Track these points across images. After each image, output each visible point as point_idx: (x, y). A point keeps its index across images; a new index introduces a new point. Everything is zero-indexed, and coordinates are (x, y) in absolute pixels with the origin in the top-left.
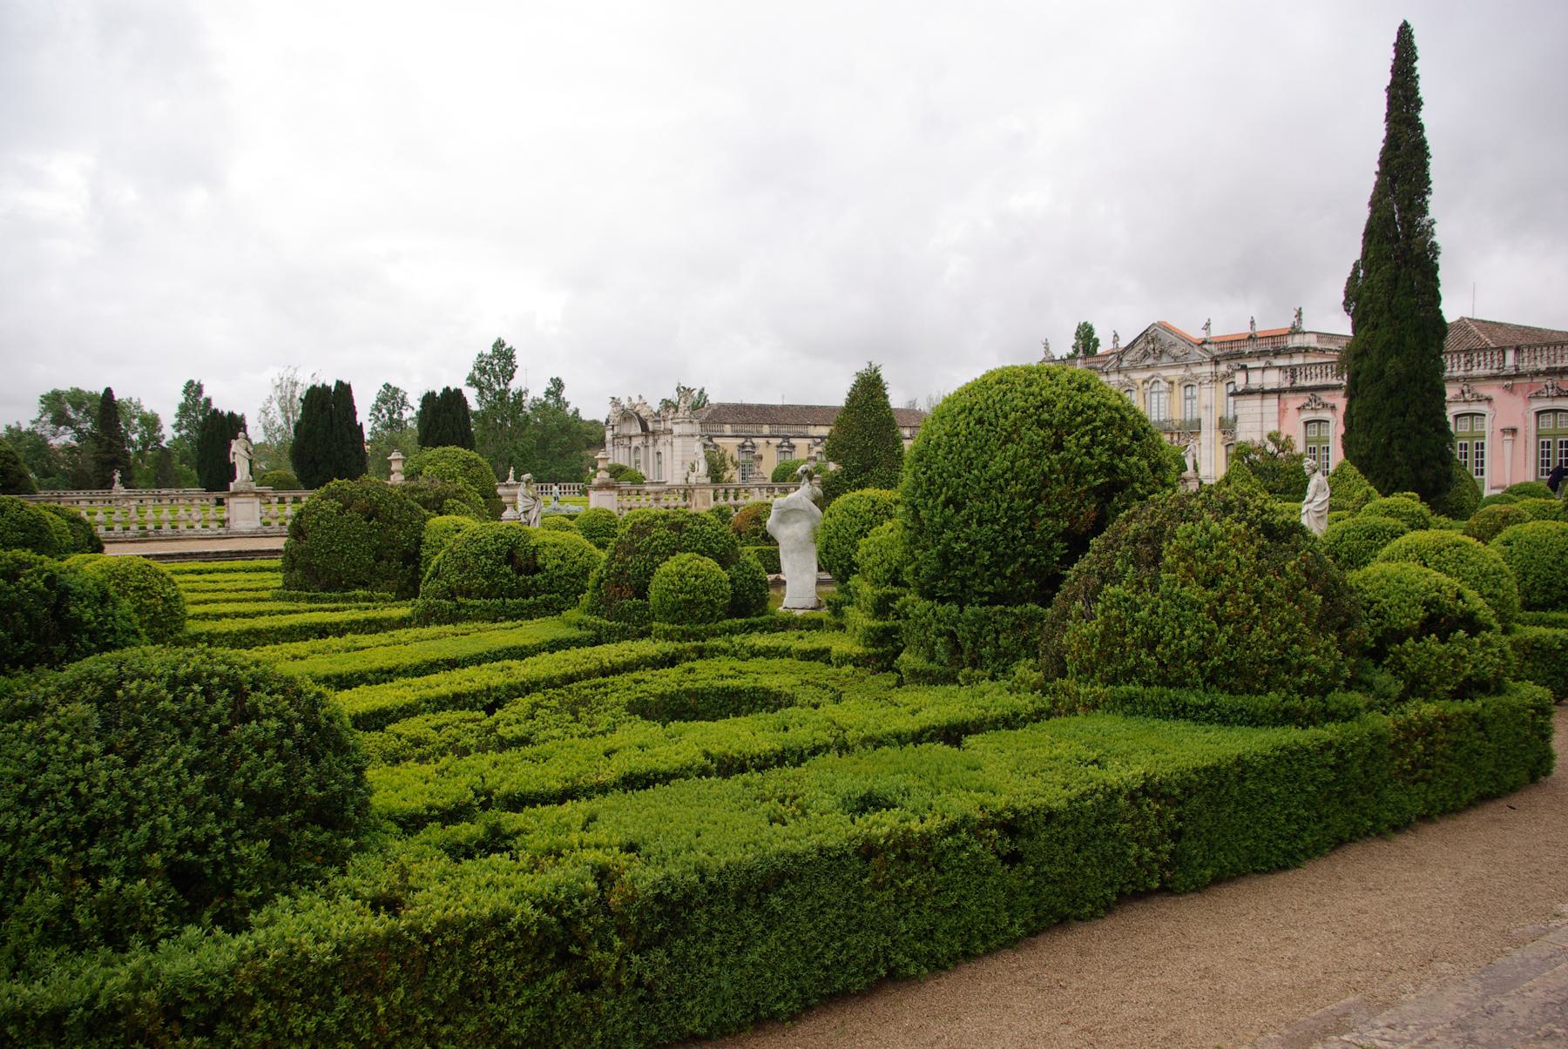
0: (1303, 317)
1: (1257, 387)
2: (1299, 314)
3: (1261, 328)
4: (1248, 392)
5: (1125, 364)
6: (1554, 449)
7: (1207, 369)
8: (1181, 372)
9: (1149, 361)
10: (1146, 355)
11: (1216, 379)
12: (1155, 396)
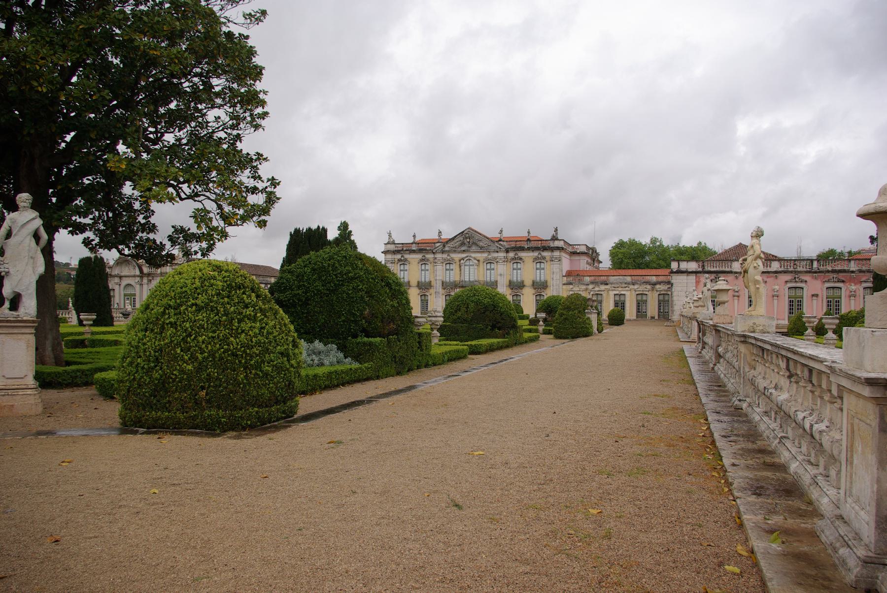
1: (685, 270)
2: (556, 230)
3: (505, 234)
5: (447, 249)
6: (833, 303)
8: (485, 255)
9: (463, 248)
10: (463, 244)
11: (506, 260)
12: (467, 268)
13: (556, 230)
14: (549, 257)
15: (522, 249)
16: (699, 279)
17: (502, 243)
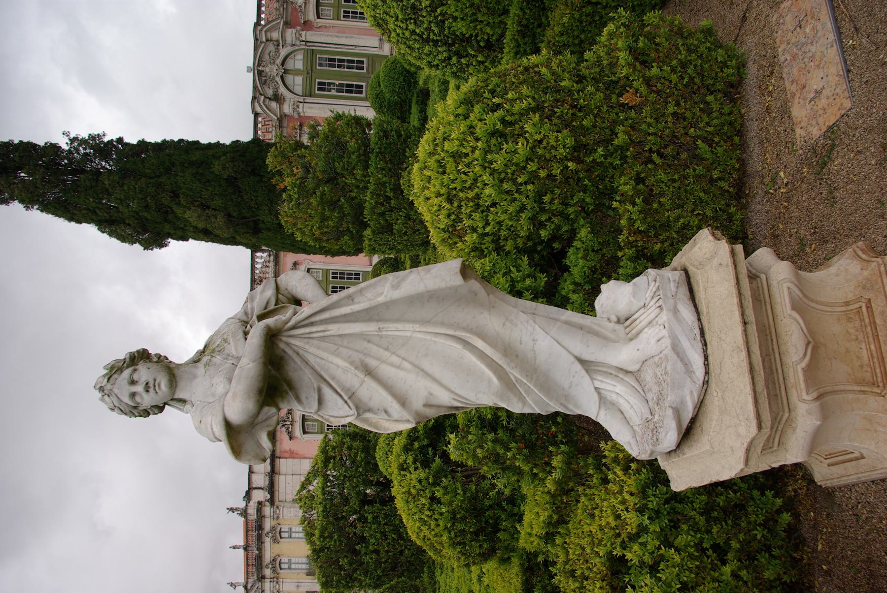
0: (234, 507)
1: (267, 478)
2: (232, 510)
4: (271, 488)
7: (267, 585)
11: (276, 579)
13: (232, 510)
14: (272, 521)
15: (259, 558)
16: (286, 452)
17: (249, 586)
